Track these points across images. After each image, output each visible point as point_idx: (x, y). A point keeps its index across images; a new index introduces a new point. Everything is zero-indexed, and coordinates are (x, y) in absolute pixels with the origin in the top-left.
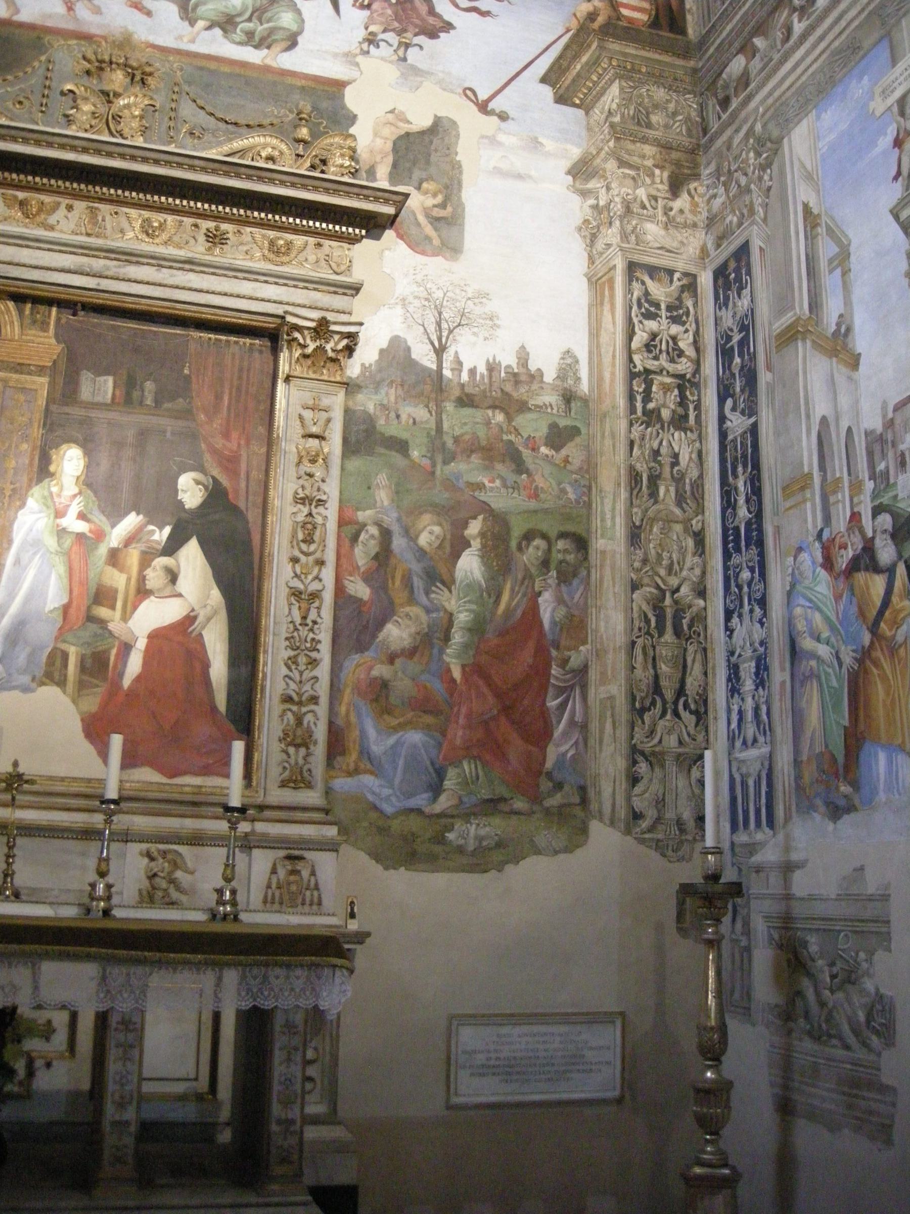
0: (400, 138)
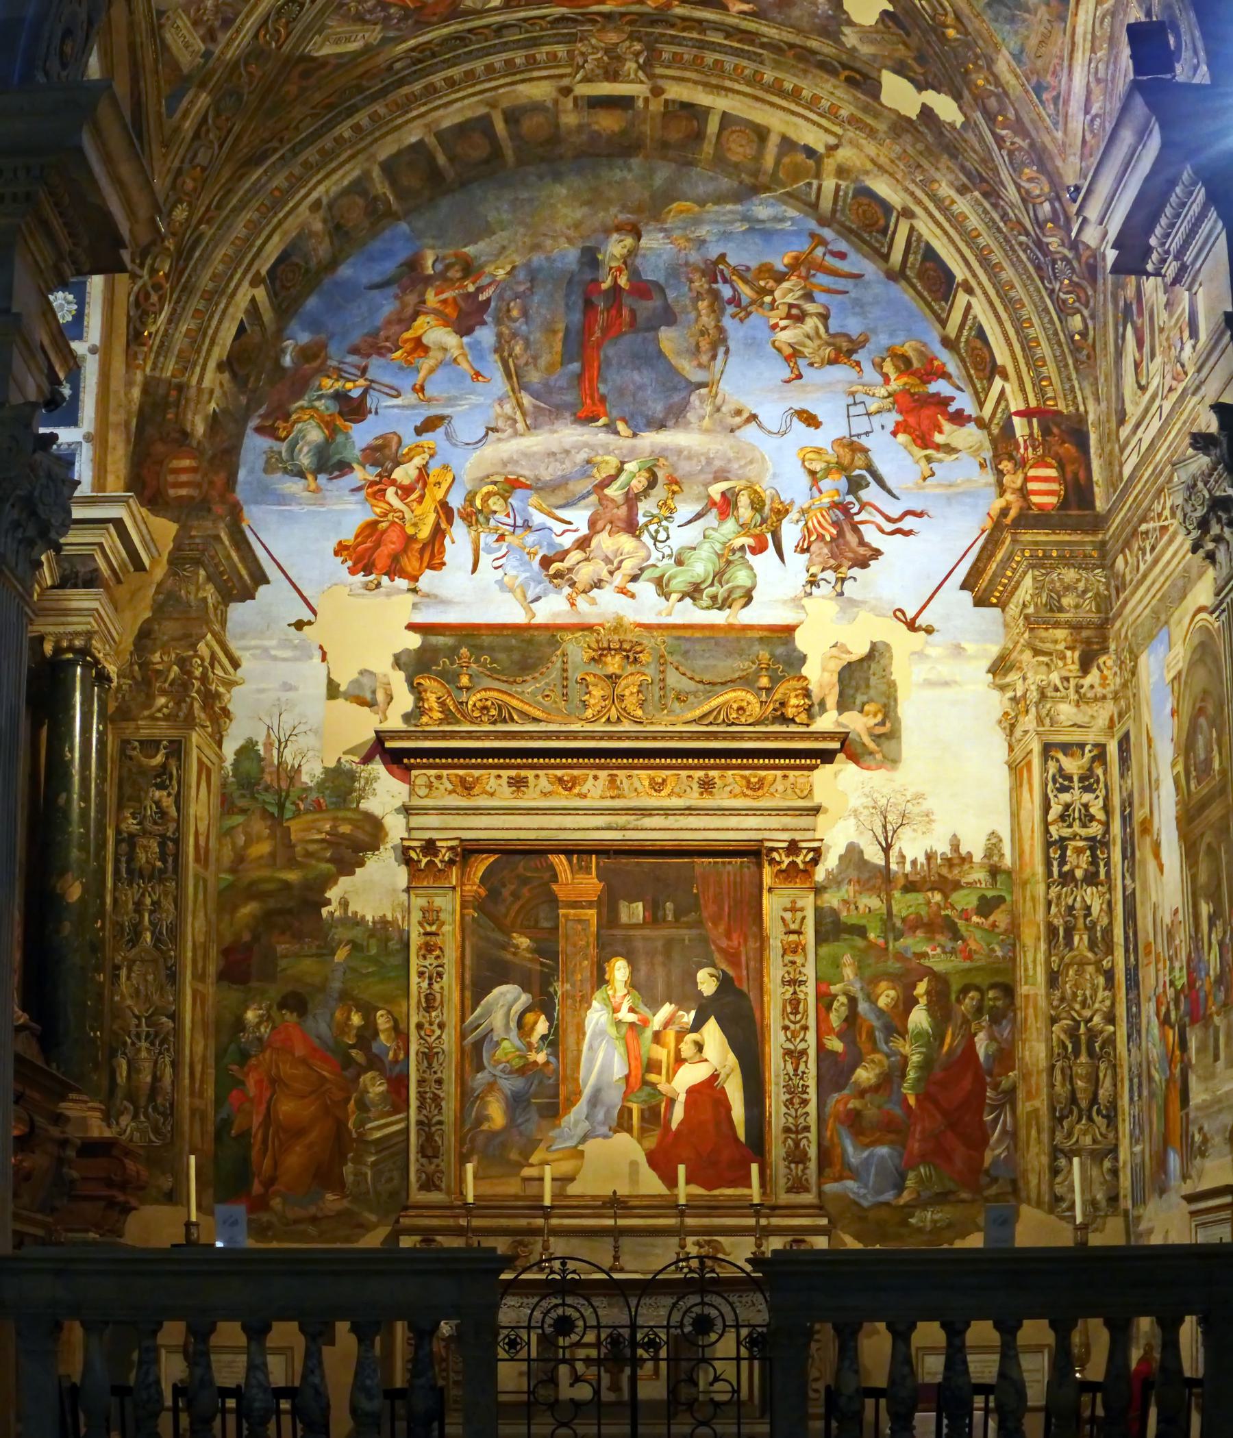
0: (844, 668)
